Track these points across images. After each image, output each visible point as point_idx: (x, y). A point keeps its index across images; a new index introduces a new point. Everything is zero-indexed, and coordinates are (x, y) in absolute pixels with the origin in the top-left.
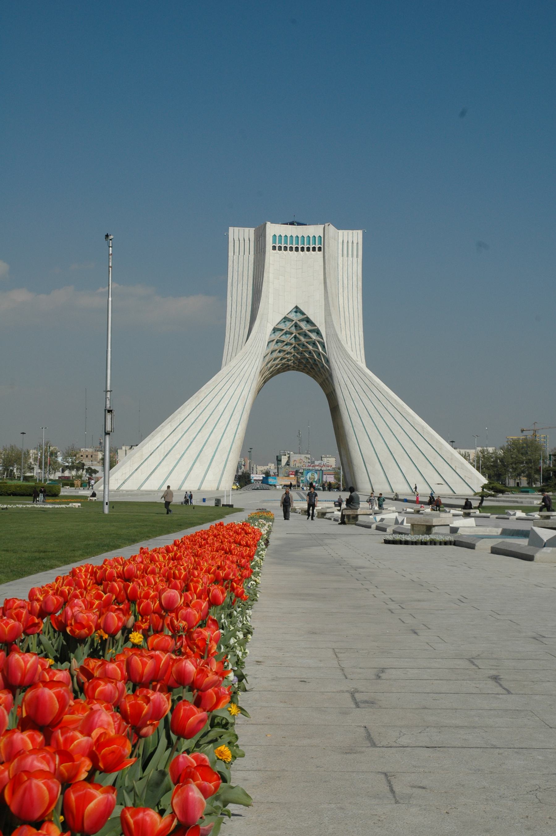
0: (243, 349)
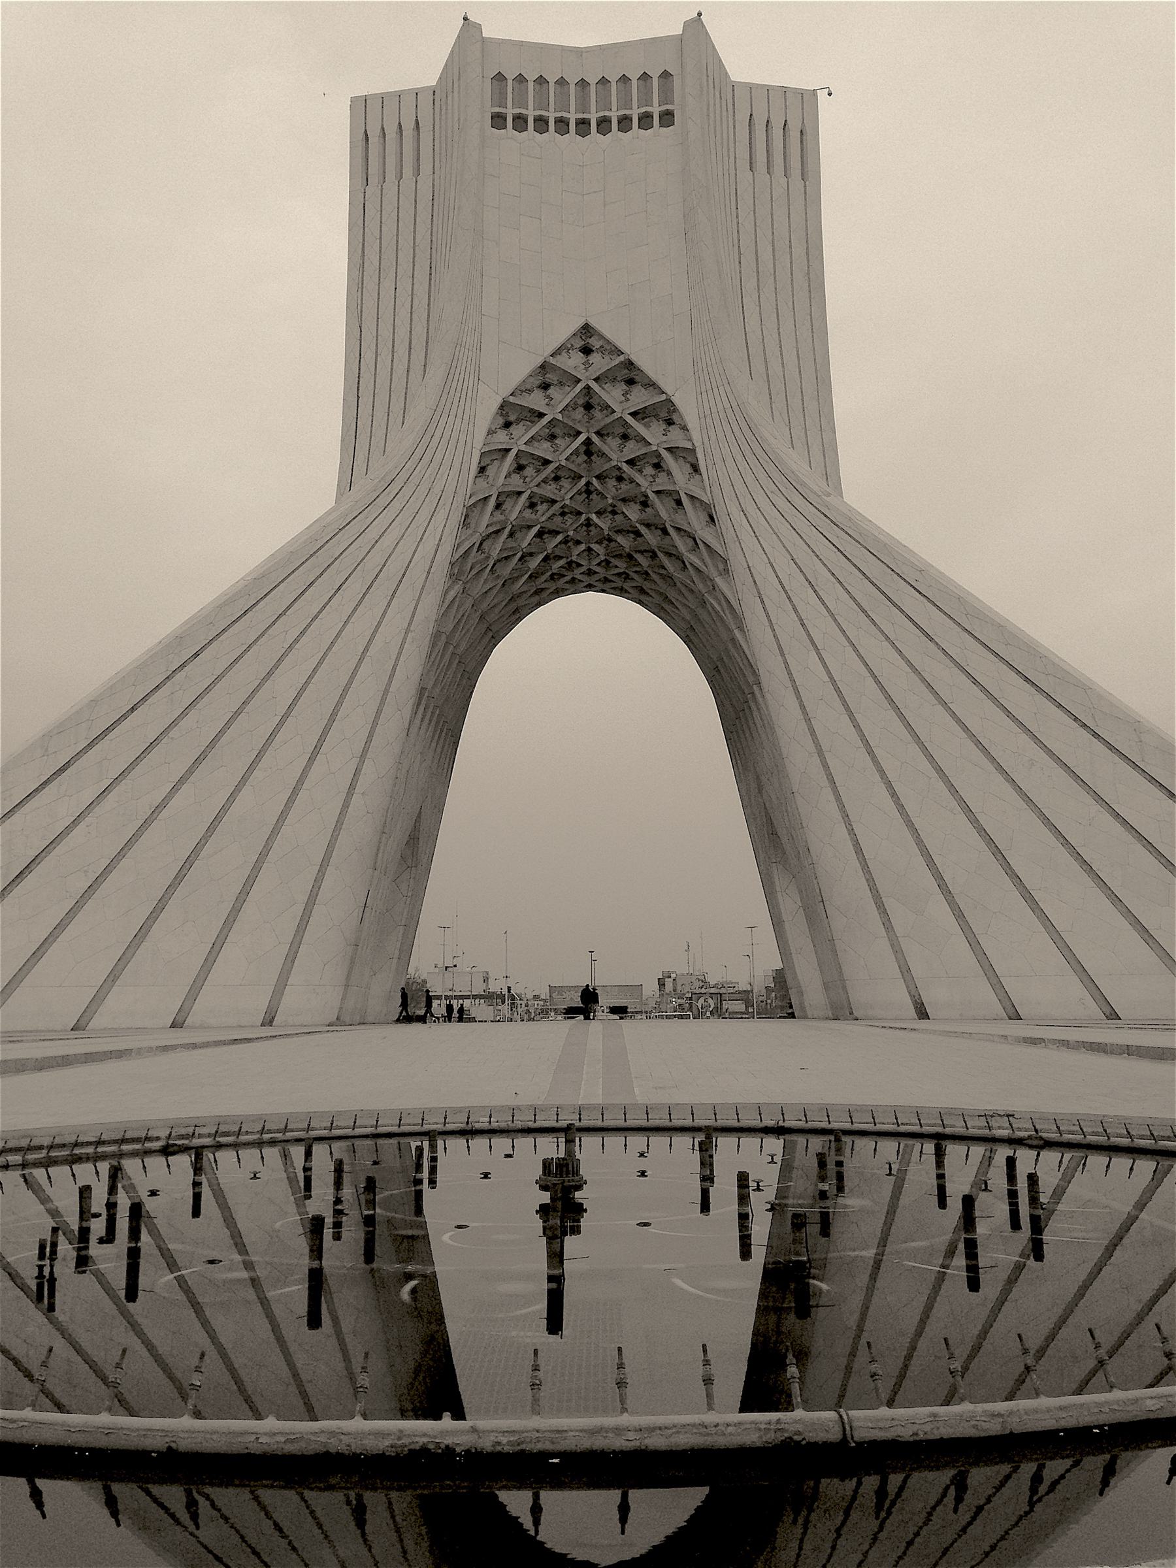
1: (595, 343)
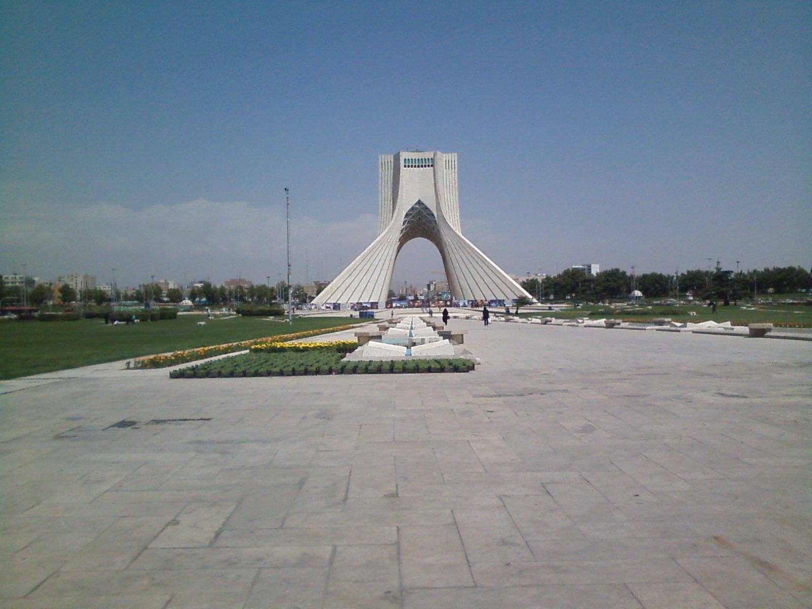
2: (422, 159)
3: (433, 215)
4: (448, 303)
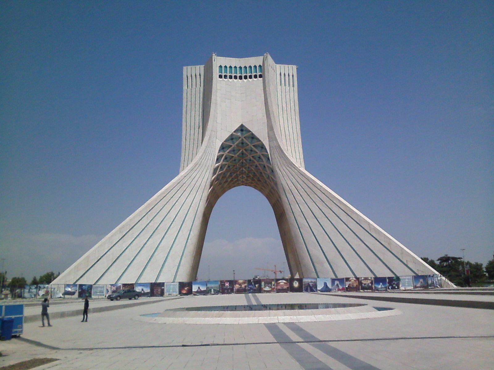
0: (193, 161)
1: (244, 128)
2: (245, 67)
3: (263, 147)
4: (296, 284)
